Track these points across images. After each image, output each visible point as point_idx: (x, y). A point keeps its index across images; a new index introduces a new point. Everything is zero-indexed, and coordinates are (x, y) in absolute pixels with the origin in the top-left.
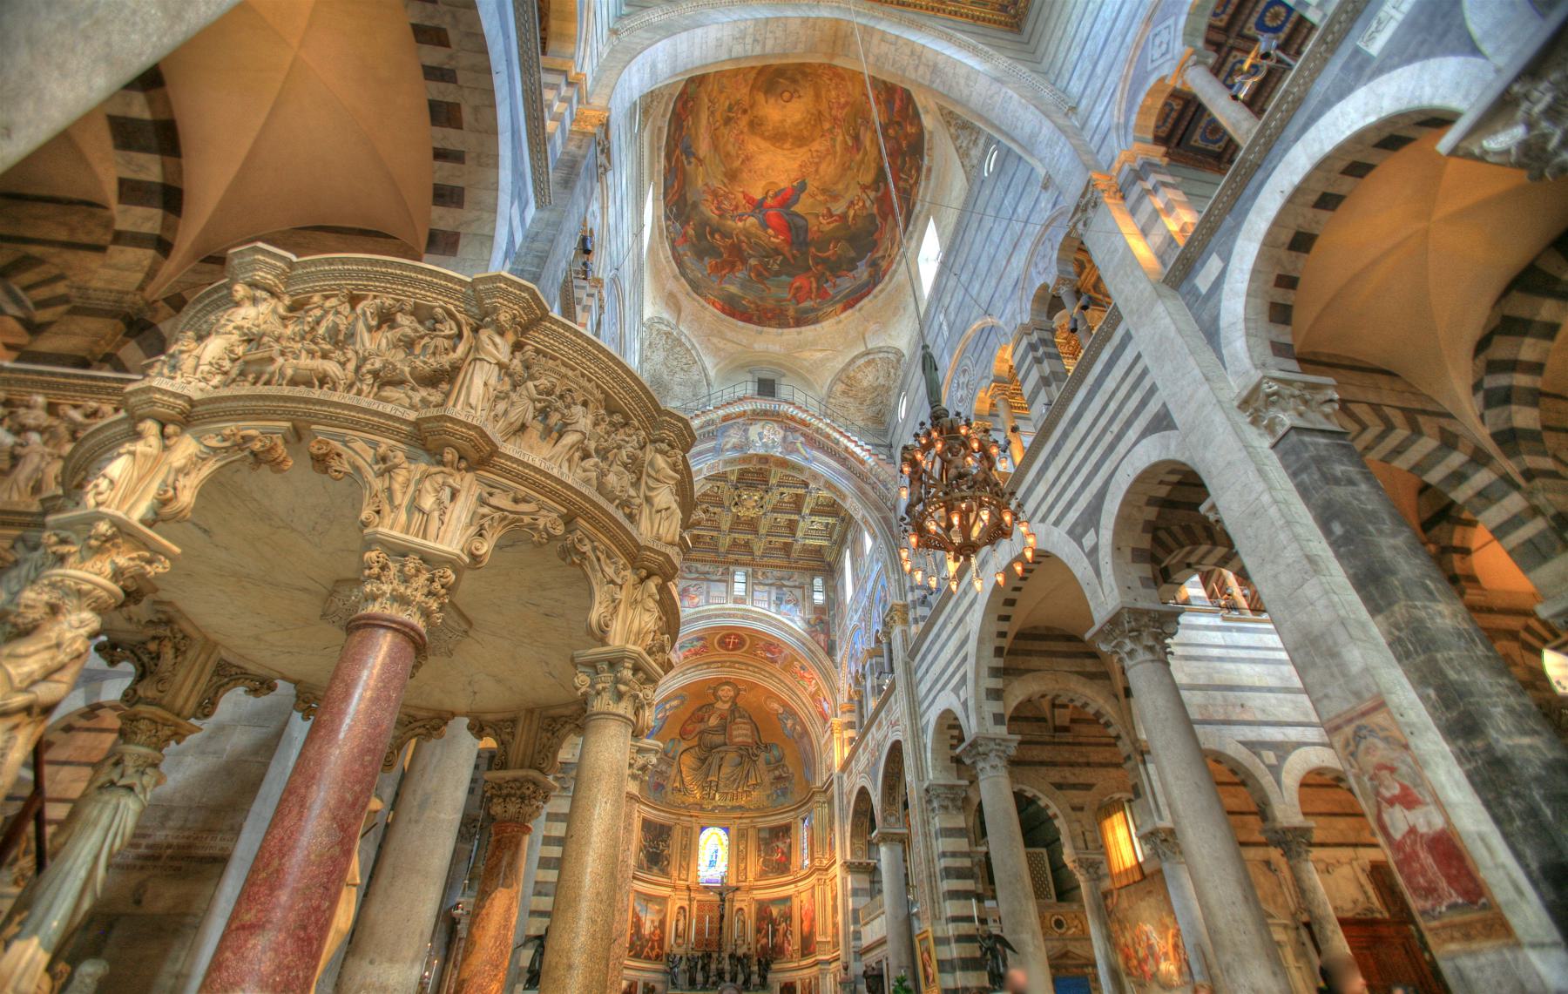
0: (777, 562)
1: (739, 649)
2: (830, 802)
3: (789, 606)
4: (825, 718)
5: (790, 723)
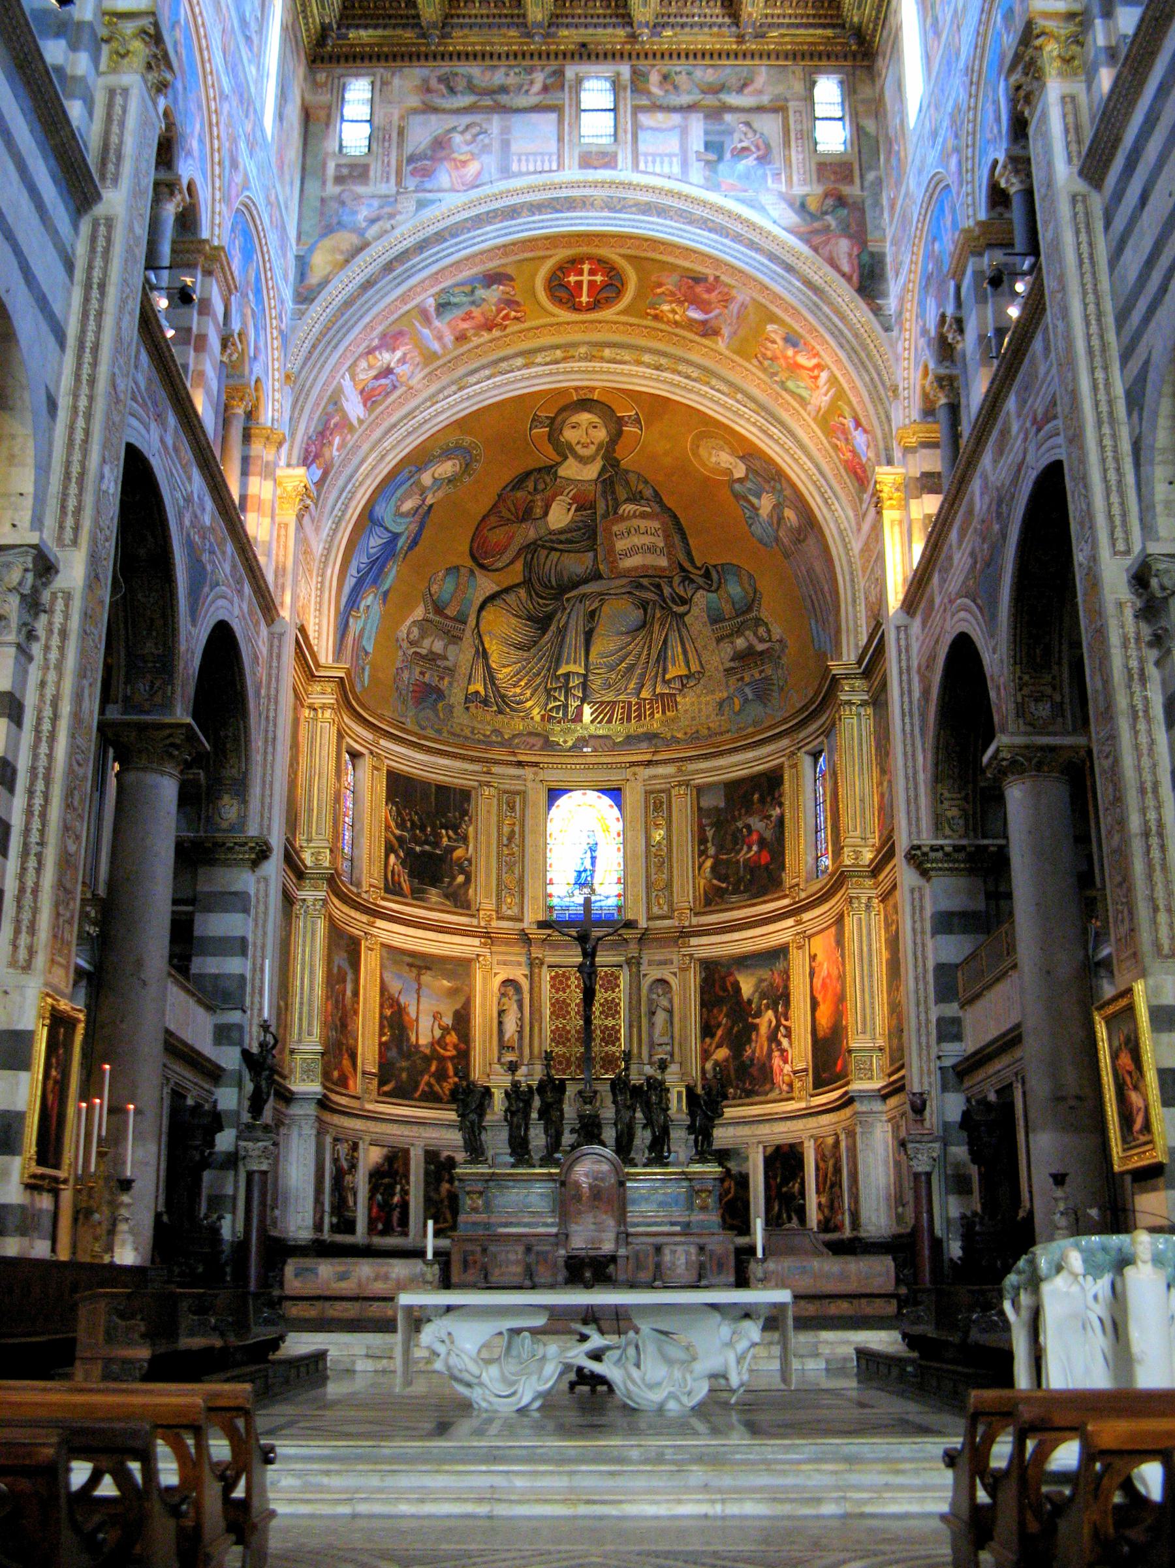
0: (704, 40)
1: (609, 302)
2: (878, 701)
3: (743, 165)
4: (860, 476)
5: (765, 504)
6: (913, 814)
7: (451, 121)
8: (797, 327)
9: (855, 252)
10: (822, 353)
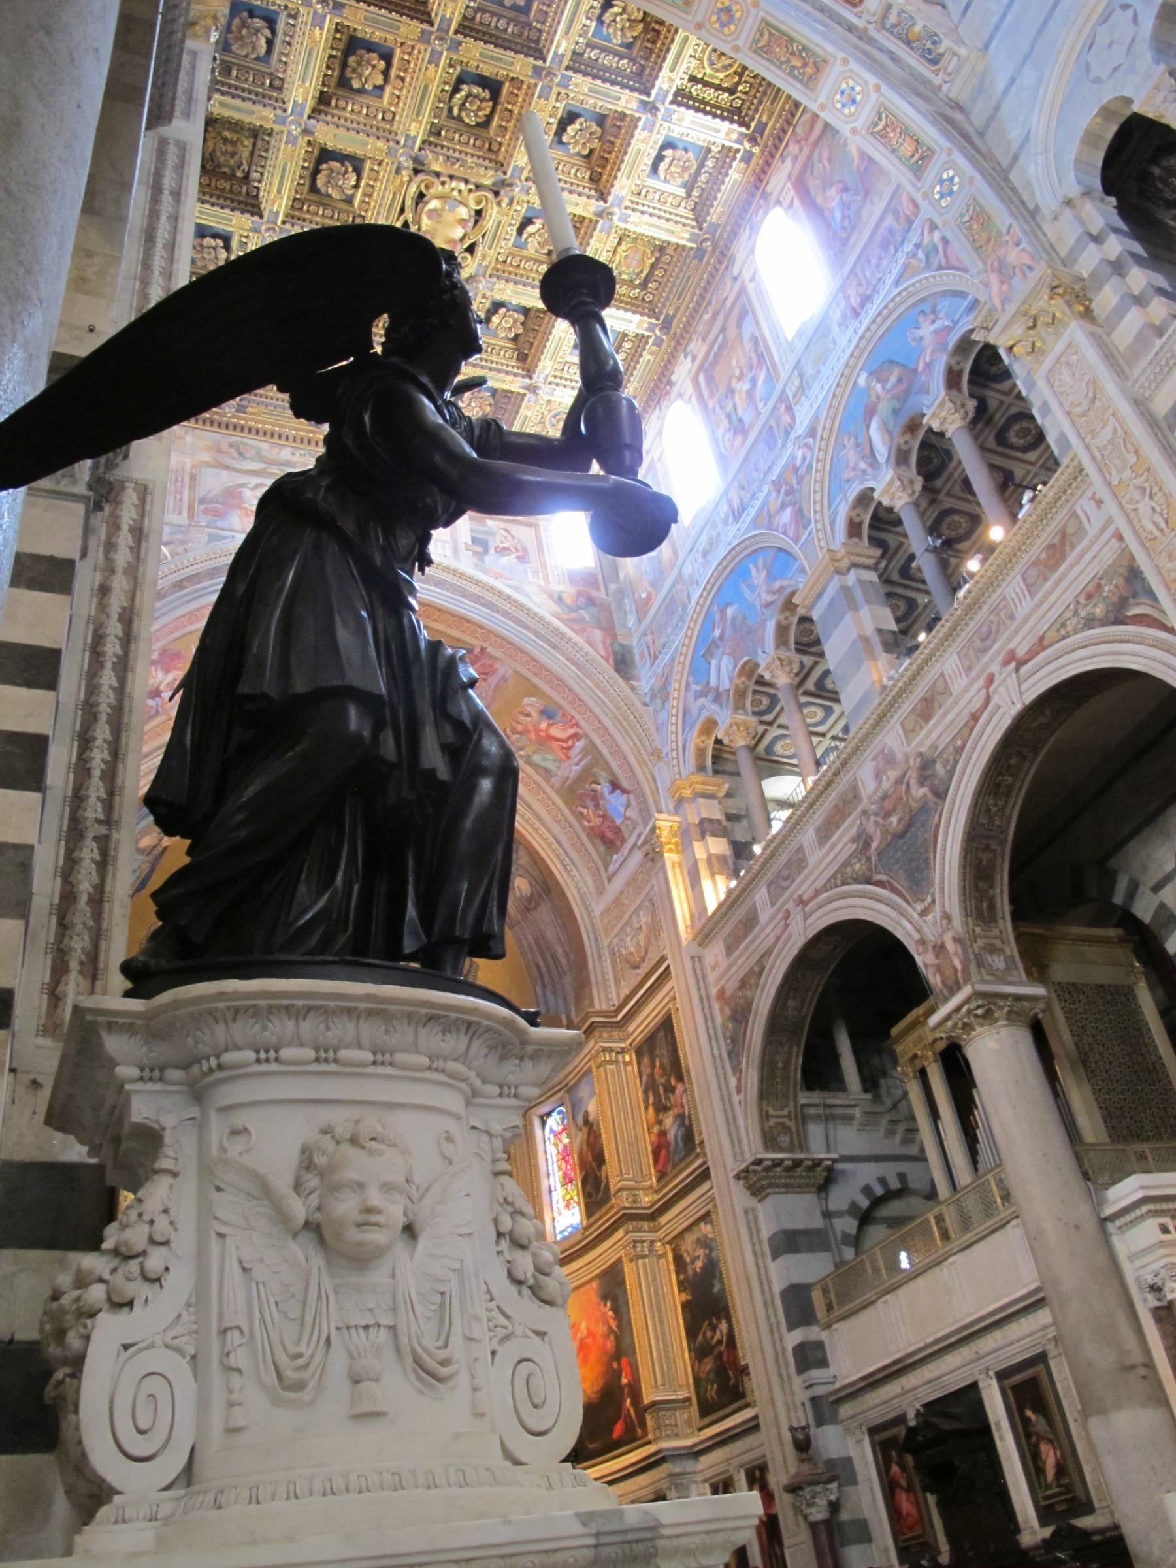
6: (734, 1136)
7: (243, 479)
8: (557, 697)
9: (608, 641)
10: (582, 723)
